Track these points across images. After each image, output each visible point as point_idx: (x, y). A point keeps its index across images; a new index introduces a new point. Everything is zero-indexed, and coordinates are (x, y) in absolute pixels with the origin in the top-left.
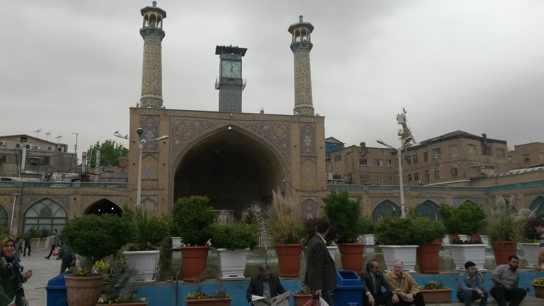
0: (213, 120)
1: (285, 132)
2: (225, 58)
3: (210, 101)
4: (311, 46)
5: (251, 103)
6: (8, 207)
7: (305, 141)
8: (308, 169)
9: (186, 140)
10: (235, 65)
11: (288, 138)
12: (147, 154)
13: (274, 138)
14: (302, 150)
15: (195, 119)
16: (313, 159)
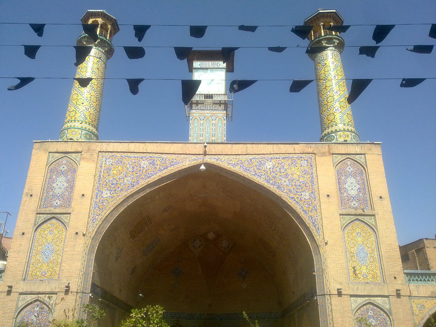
0: (174, 156)
1: (305, 172)
9: (122, 190)
11: (312, 182)
12: (49, 216)
13: (285, 182)
14: (344, 201)
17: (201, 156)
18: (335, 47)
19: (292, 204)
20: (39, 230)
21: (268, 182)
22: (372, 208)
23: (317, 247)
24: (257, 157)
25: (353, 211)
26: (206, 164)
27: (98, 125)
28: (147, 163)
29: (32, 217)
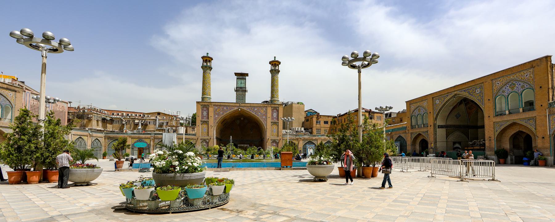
3: (231, 97)
4: (279, 71)
5: (250, 98)
10: (243, 81)
13: (259, 114)
14: (272, 119)
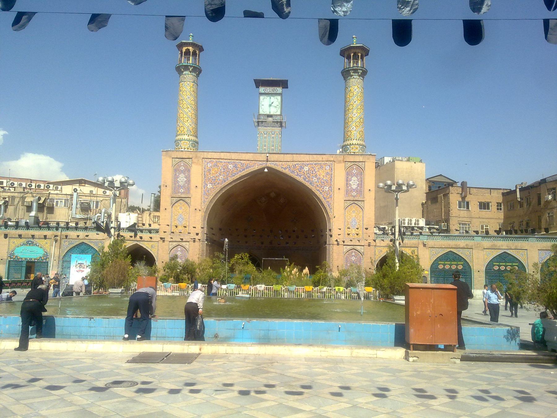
0: (248, 162)
1: (327, 174)
2: (263, 92)
6: (49, 250)
7: (351, 182)
8: (354, 215)
11: (331, 180)
14: (348, 192)
15: (229, 161)
16: (359, 203)
17: (264, 162)
18: (359, 76)
19: (318, 193)
20: (174, 207)
21: (305, 180)
22: (364, 197)
23: (329, 219)
24: (299, 163)
25: (352, 198)
26: (268, 168)
27: (197, 132)
28: (232, 166)
29: (169, 199)
